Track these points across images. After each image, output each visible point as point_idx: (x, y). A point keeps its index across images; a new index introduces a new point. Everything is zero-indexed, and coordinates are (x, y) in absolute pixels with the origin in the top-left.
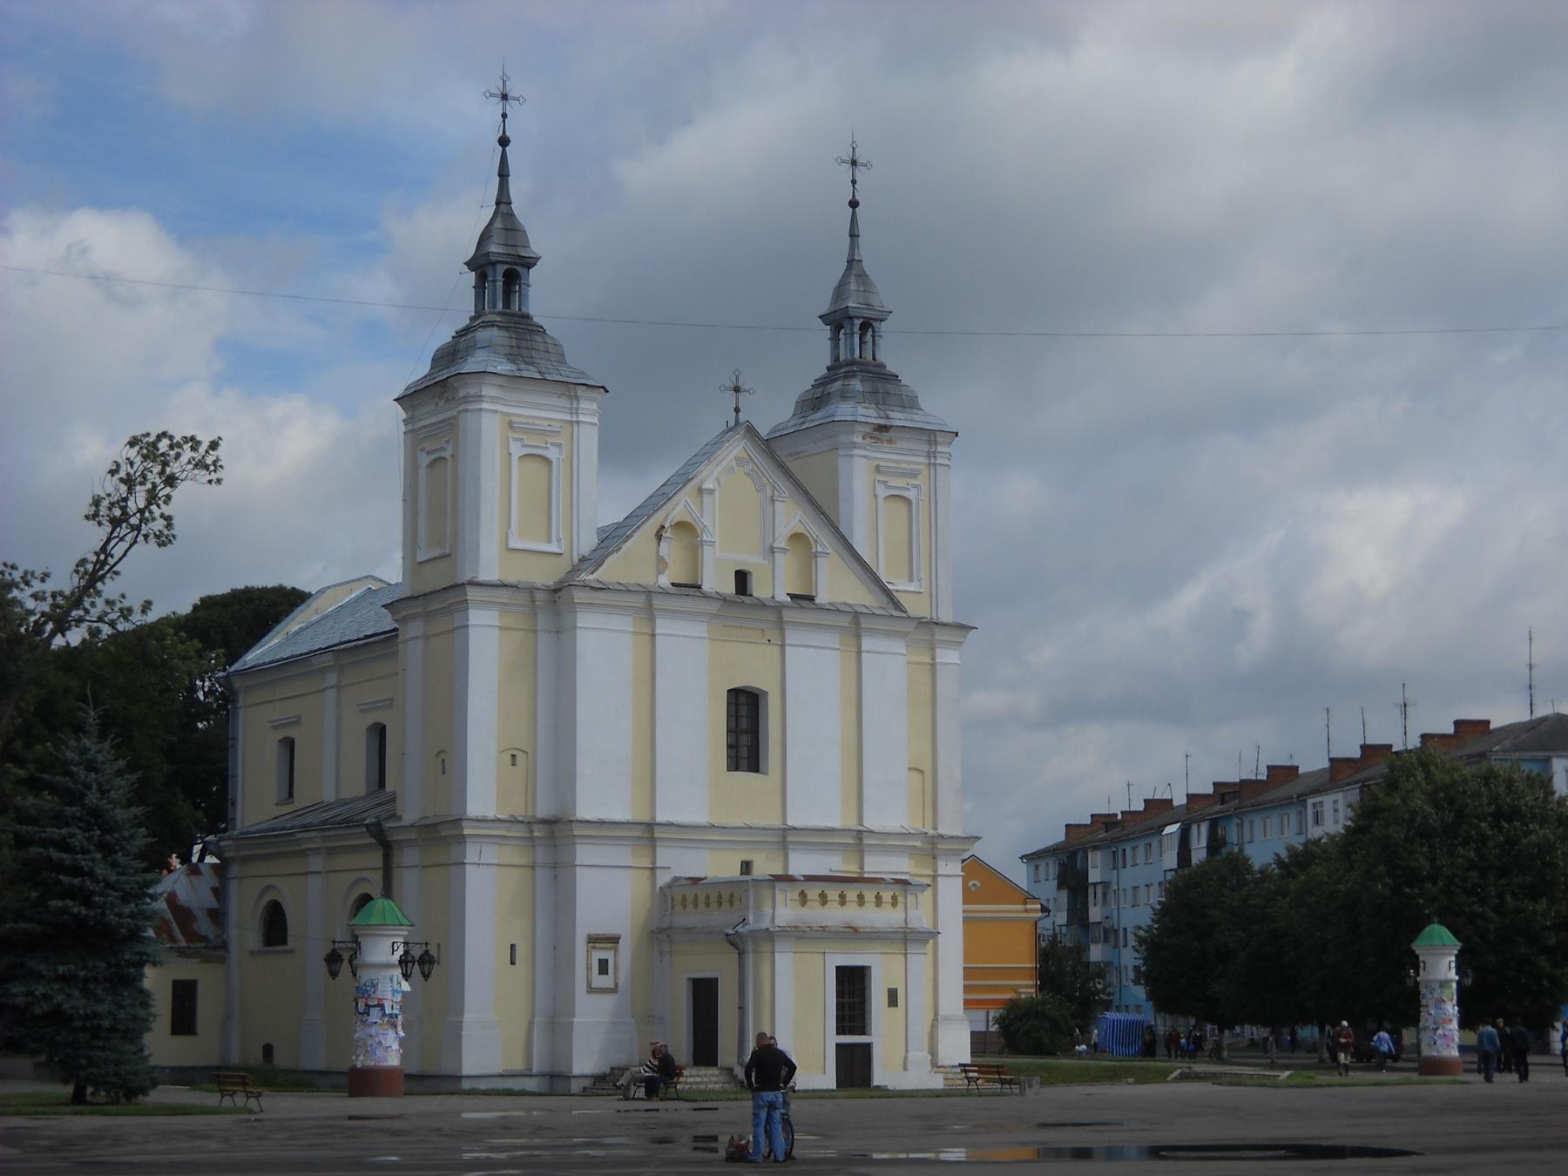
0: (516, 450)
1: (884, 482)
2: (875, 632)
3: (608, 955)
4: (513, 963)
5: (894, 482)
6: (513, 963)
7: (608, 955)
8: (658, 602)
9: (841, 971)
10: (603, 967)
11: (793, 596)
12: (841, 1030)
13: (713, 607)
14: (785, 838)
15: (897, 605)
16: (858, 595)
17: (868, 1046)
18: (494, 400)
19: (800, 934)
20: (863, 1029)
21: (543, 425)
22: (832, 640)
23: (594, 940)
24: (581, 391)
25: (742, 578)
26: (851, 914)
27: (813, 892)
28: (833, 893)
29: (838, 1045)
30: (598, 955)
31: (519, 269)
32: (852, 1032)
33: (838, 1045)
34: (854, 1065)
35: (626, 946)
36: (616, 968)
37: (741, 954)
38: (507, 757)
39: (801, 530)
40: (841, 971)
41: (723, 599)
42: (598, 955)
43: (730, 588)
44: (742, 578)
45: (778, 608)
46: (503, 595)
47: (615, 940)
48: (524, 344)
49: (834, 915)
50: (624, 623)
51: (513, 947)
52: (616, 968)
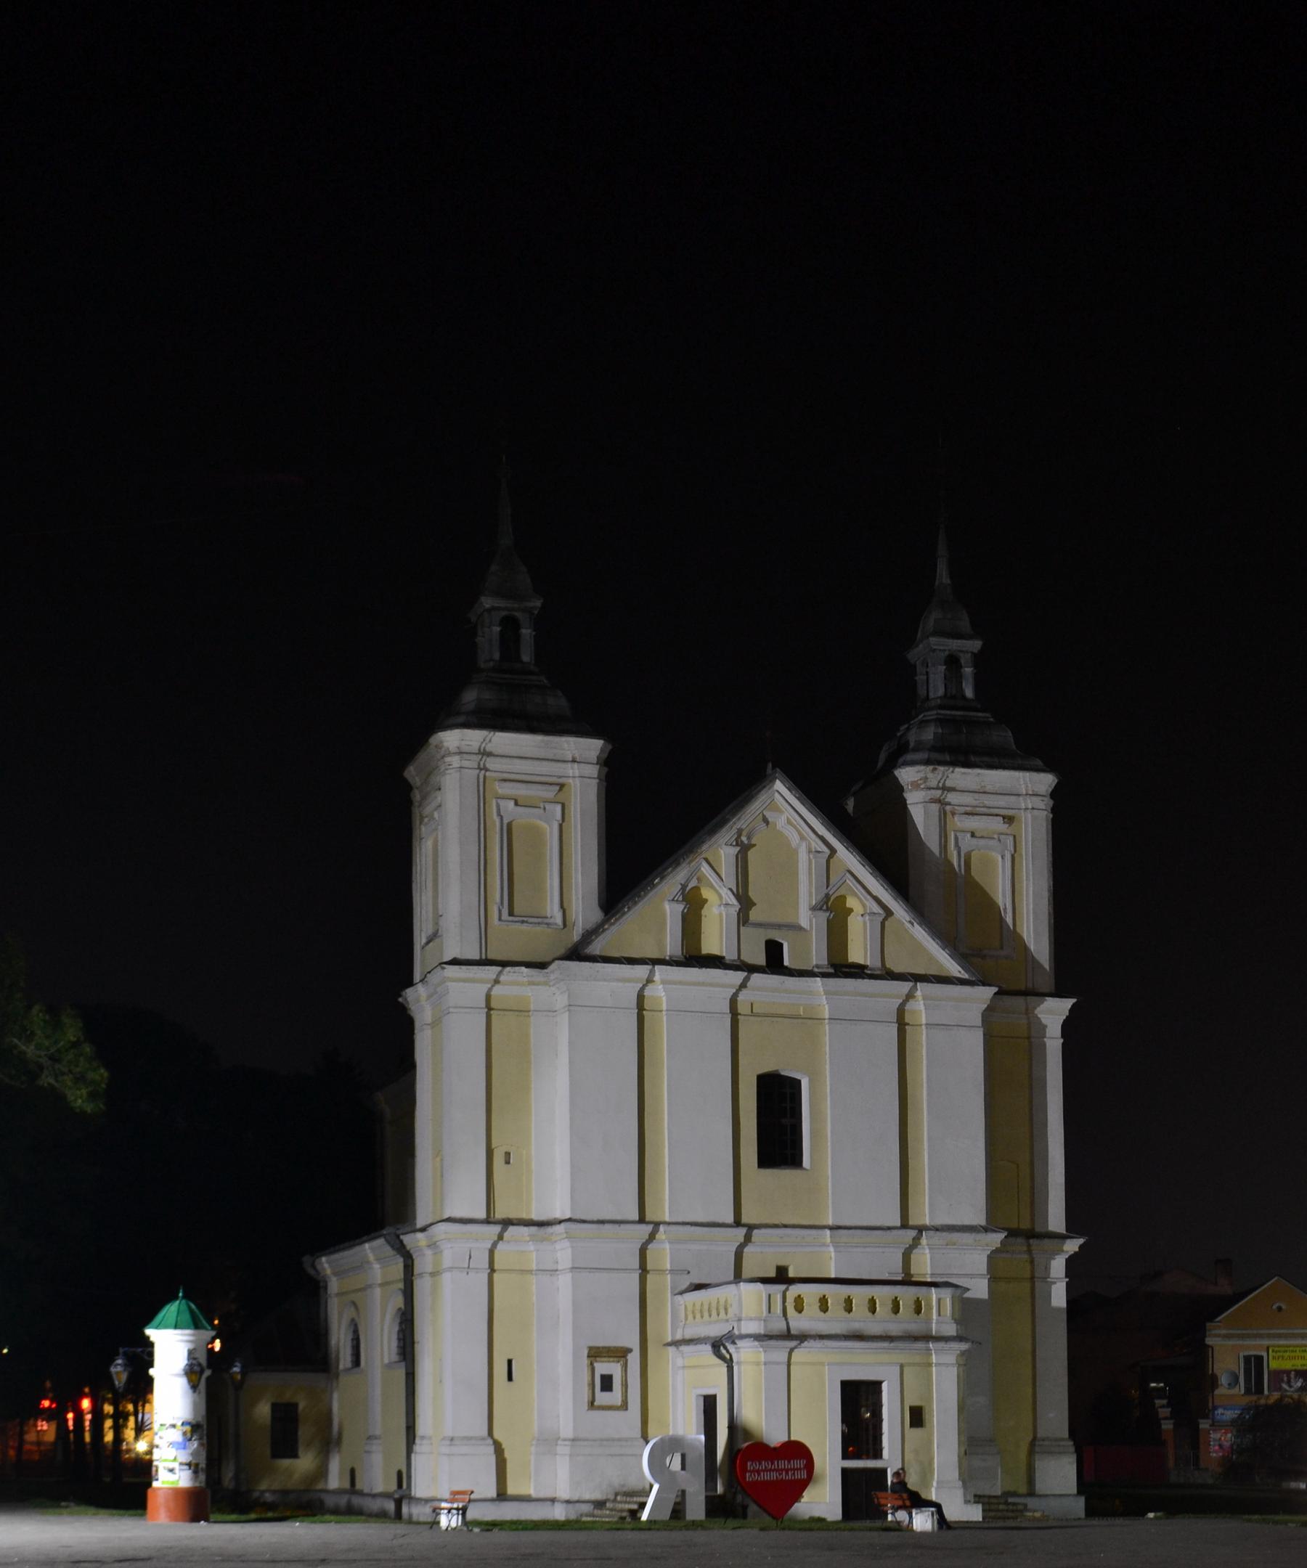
3: (614, 1368)
4: (510, 1378)
6: (510, 1378)
10: (607, 1383)
23: (596, 1354)
25: (774, 950)
35: (634, 1359)
36: (625, 1385)
42: (603, 1368)
43: (761, 960)
44: (774, 950)
47: (620, 1354)
51: (510, 1362)
52: (625, 1385)
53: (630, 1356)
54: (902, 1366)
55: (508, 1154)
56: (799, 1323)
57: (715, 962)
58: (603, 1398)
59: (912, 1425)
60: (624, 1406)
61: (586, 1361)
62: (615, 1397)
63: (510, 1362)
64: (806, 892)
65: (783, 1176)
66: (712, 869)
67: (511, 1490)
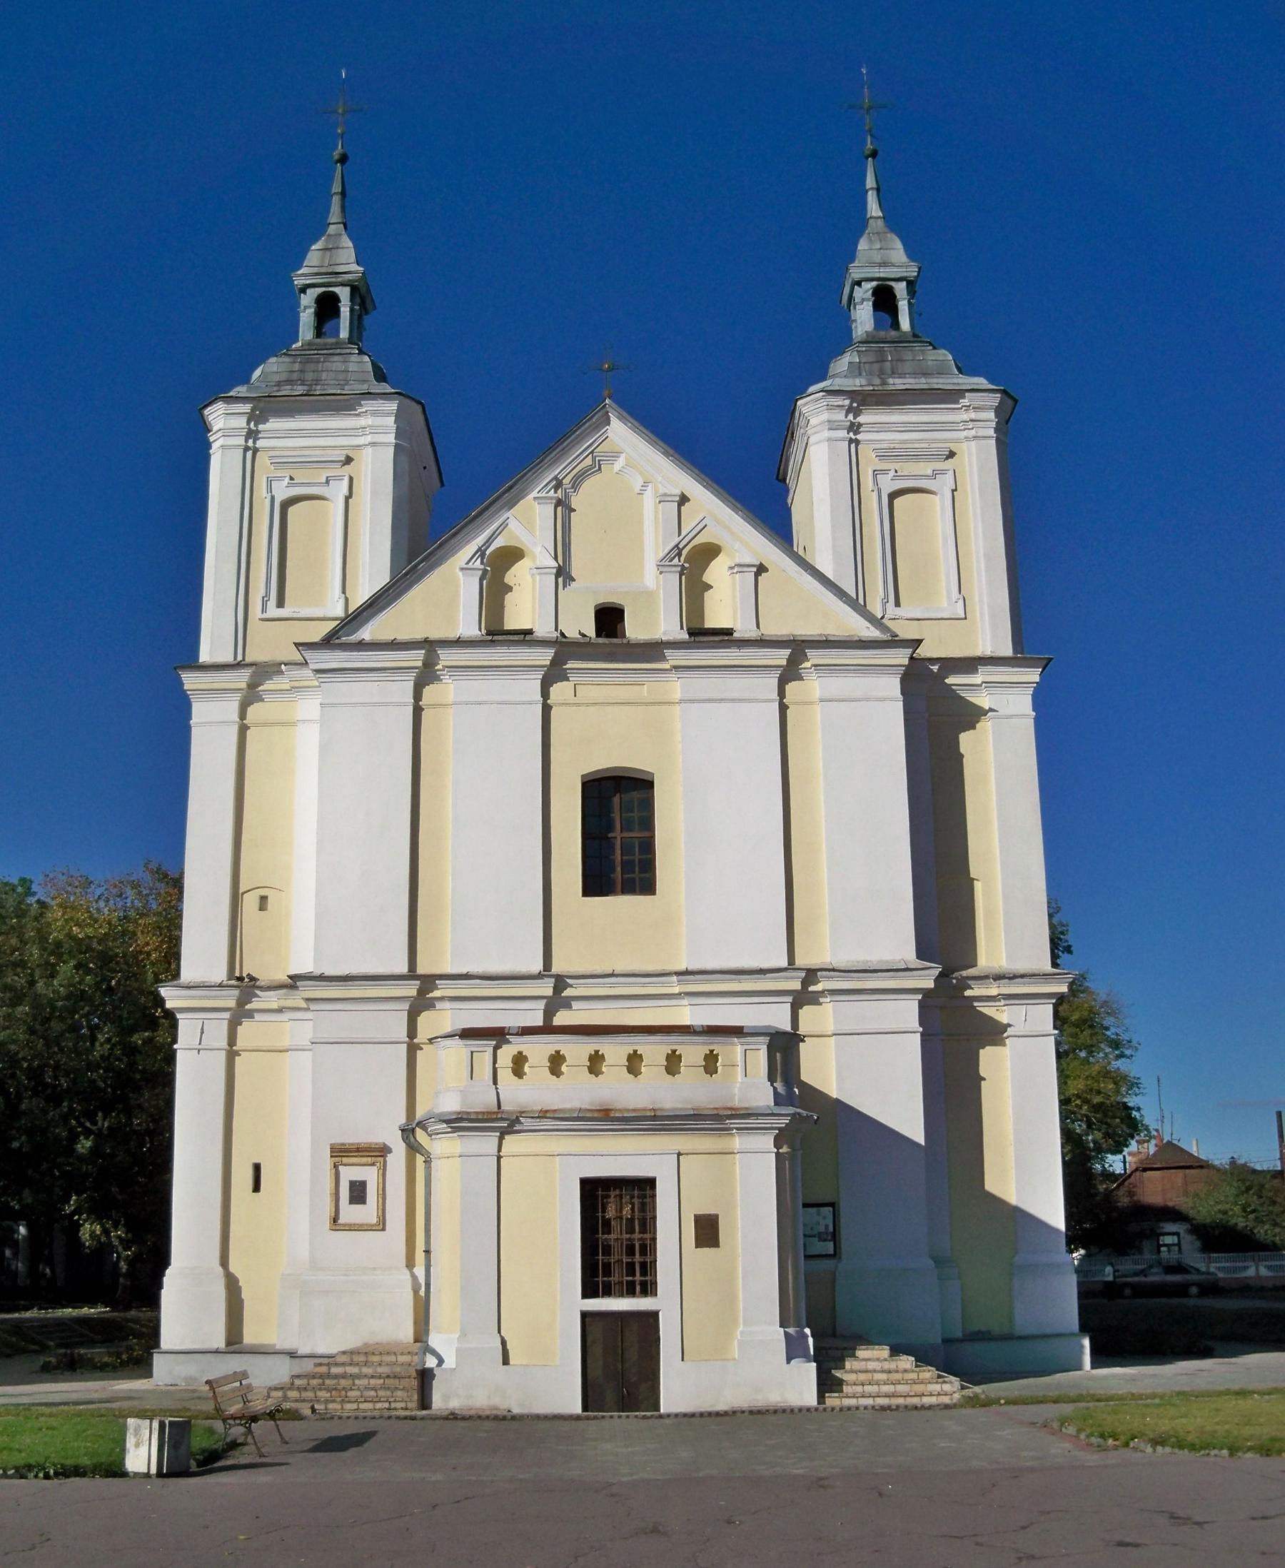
3: (369, 1175)
6: (257, 1188)
7: (369, 1175)
8: (447, 657)
9: (595, 1193)
10: (358, 1193)
12: (589, 1290)
17: (654, 1316)
19: (502, 1123)
20: (648, 1288)
21: (316, 455)
23: (341, 1152)
25: (609, 619)
29: (585, 1315)
30: (350, 1173)
31: (336, 290)
33: (585, 1315)
40: (595, 1193)
42: (350, 1173)
44: (609, 619)
48: (311, 367)
51: (257, 1168)
53: (390, 1158)
54: (679, 1154)
55: (264, 899)
56: (516, 1093)
57: (525, 637)
58: (350, 1213)
59: (699, 1244)
60: (381, 1225)
61: (327, 1163)
62: (367, 1214)
63: (257, 1168)
64: (654, 541)
65: (619, 907)
66: (527, 522)
67: (249, 1338)
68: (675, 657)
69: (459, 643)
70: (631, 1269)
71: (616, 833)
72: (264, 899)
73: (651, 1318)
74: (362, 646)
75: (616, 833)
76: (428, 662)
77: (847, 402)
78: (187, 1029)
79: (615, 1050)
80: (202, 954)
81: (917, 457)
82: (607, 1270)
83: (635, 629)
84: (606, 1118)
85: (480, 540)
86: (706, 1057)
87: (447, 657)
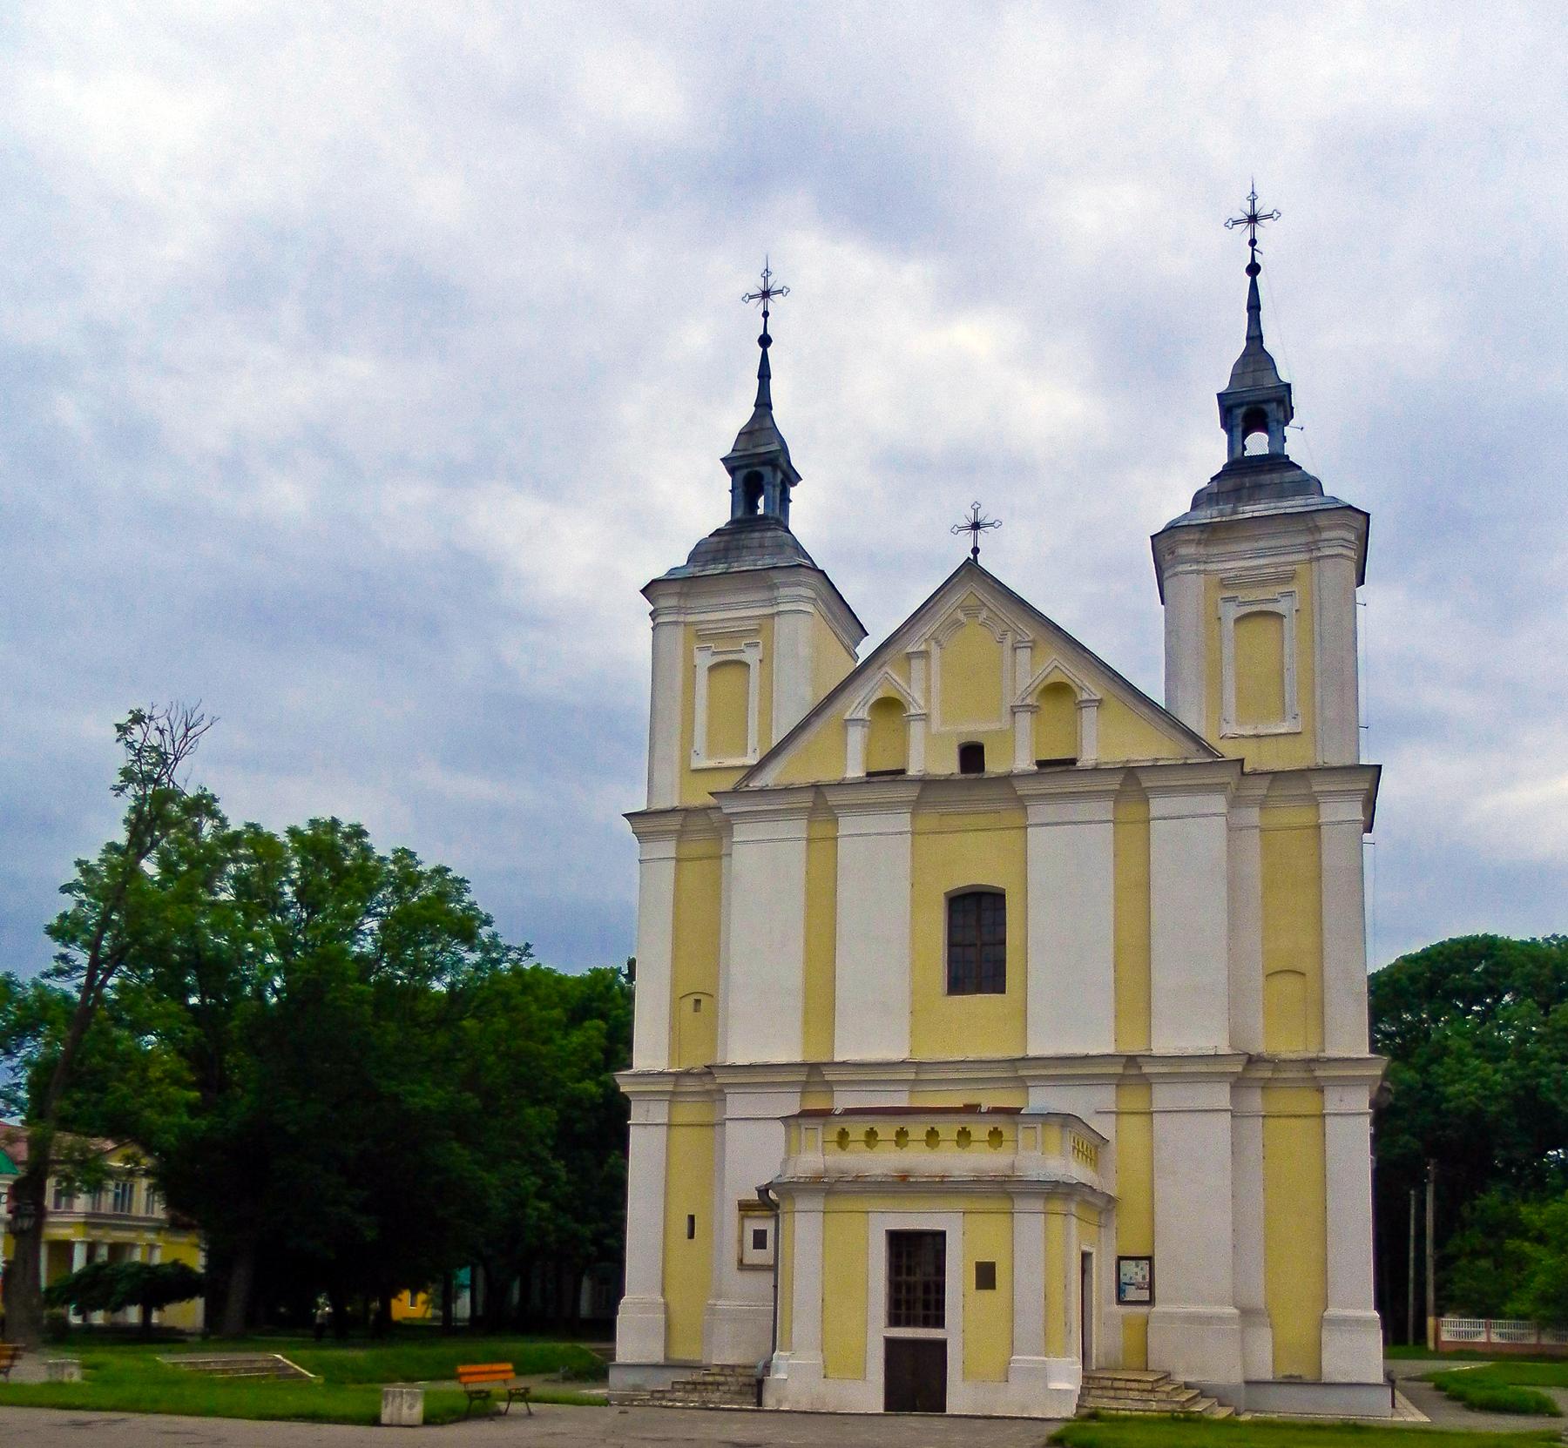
0: (703, 661)
1: (1233, 599)
2: (1168, 791)
5: (1243, 595)
8: (833, 798)
11: (1040, 764)
13: (912, 793)
14: (1021, 1070)
15: (1207, 749)
16: (1143, 745)
18: (679, 610)
19: (826, 1187)
20: (939, 1322)
22: (1104, 809)
24: (778, 577)
25: (972, 755)
26: (918, 1159)
27: (857, 1129)
28: (886, 1129)
32: (909, 1322)
34: (916, 1379)
37: (777, 1216)
38: (690, 1001)
39: (1056, 677)
41: (928, 783)
44: (972, 755)
45: (1007, 779)
46: (674, 823)
49: (884, 1160)
50: (797, 828)
55: (698, 1002)
68: (1023, 789)
69: (842, 785)
70: (926, 1306)
71: (976, 943)
72: (698, 1002)
73: (941, 1345)
74: (762, 791)
75: (976, 943)
76: (820, 802)
77: (1197, 536)
78: (637, 1114)
79: (917, 1130)
80: (650, 1049)
81: (1263, 583)
82: (910, 1305)
83: (994, 765)
84: (903, 1185)
85: (863, 694)
86: (959, 1133)
87: (833, 798)
